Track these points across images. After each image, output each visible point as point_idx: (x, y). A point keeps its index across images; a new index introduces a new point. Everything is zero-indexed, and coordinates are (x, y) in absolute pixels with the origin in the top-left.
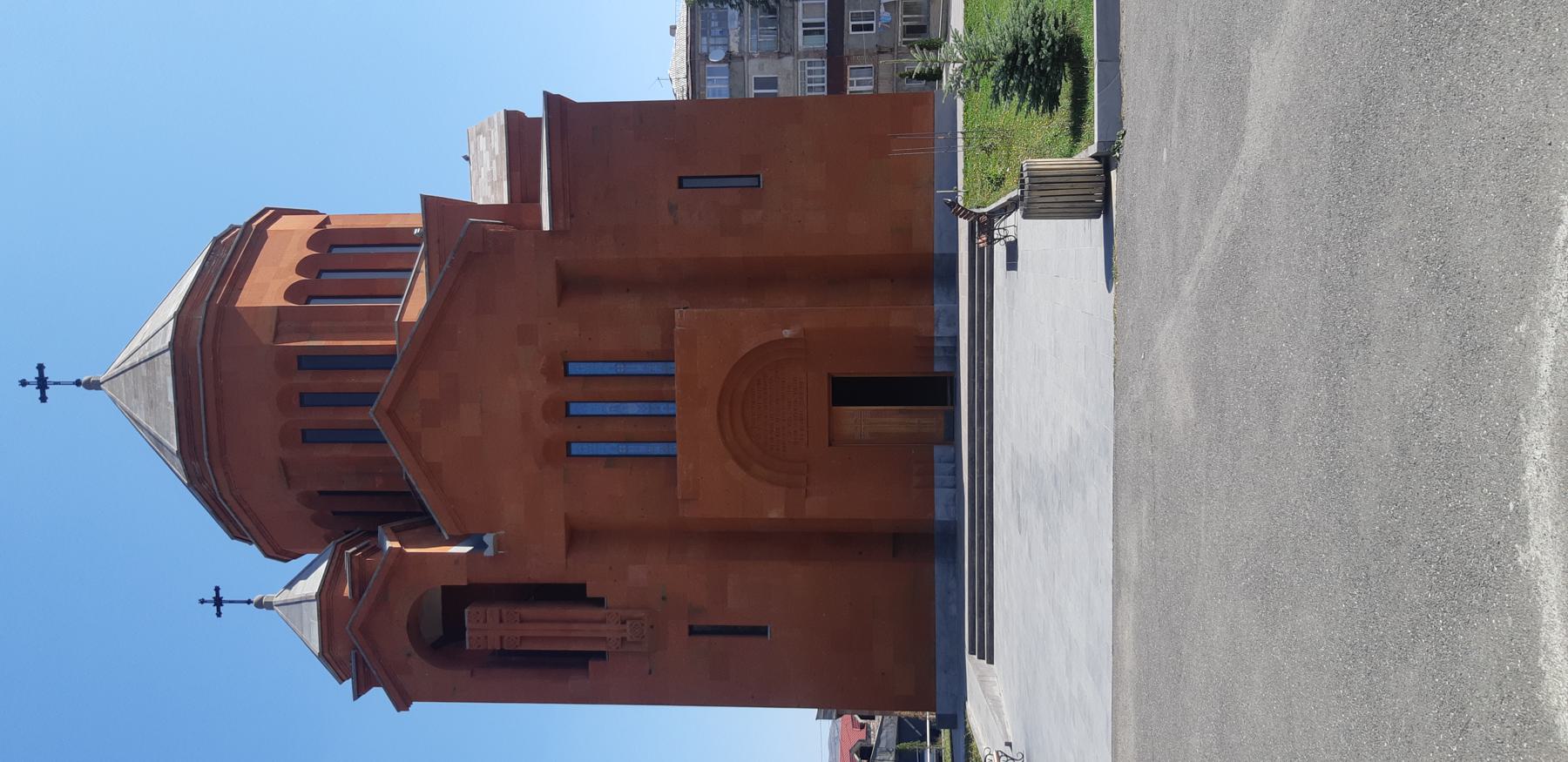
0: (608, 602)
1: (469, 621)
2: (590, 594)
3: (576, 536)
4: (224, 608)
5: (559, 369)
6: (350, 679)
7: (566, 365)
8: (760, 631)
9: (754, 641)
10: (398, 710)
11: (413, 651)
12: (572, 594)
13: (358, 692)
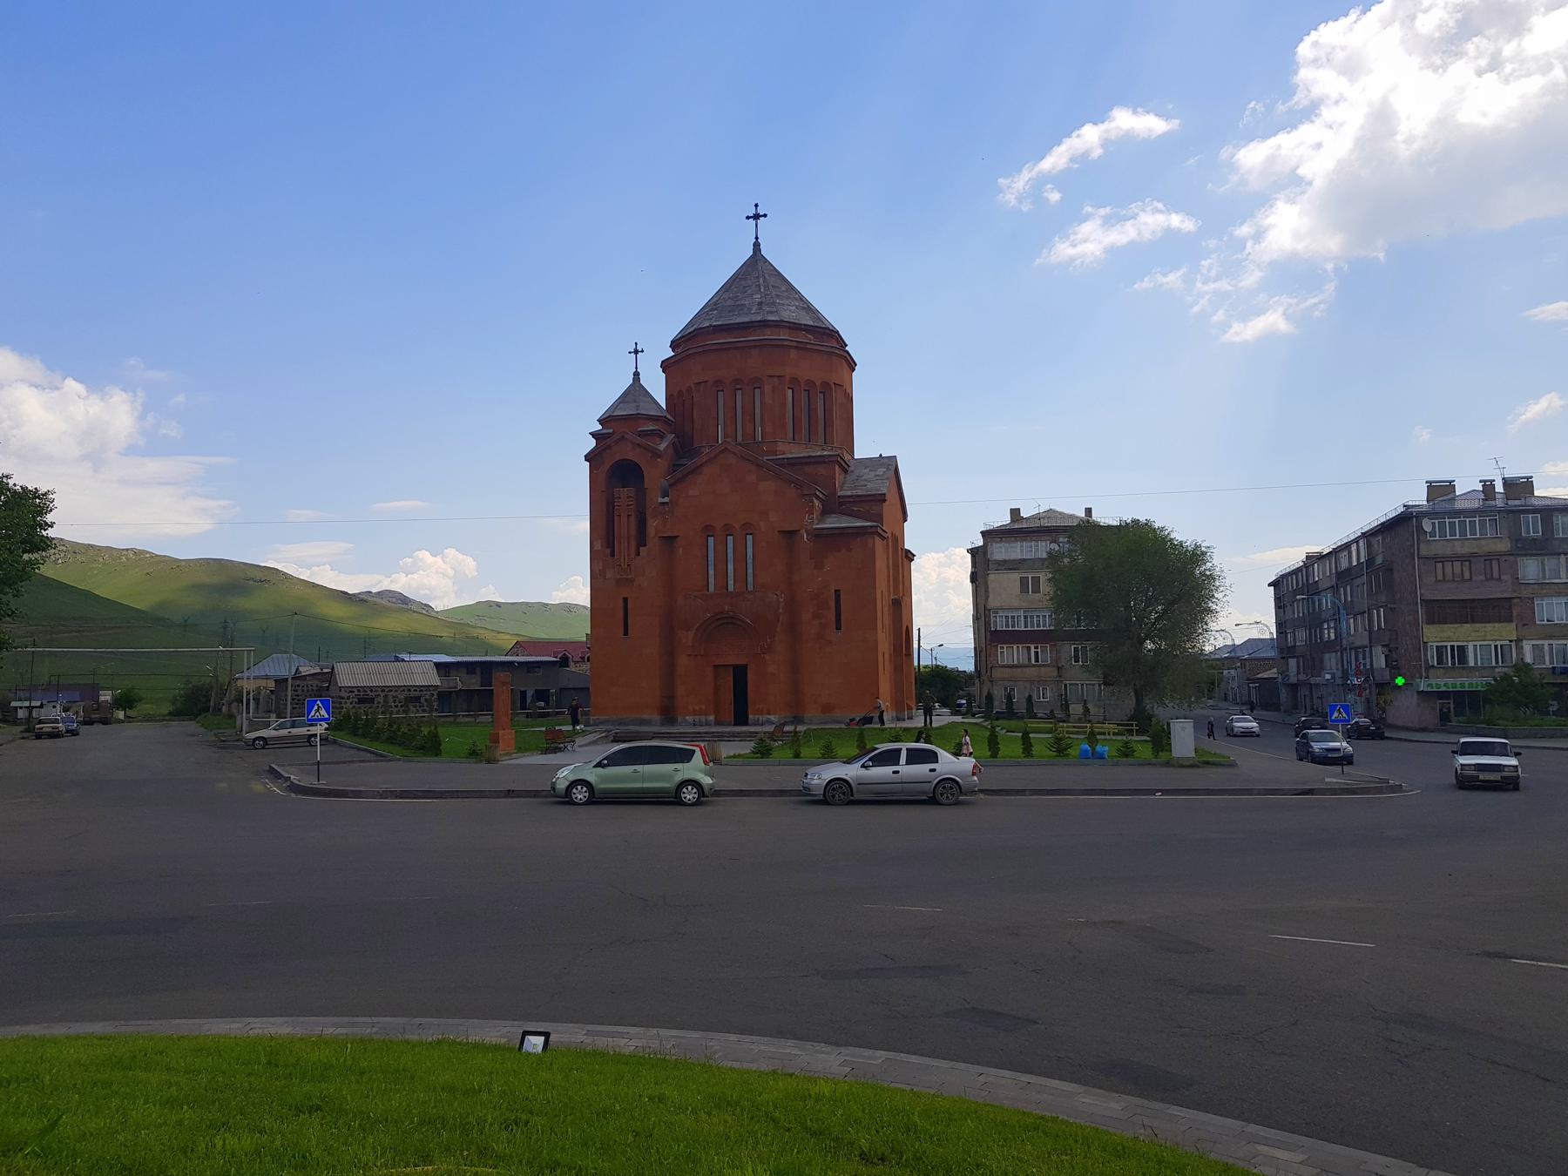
0: (638, 557)
3: (670, 540)
5: (748, 528)
6: (601, 427)
8: (626, 633)
12: (642, 540)
13: (593, 435)
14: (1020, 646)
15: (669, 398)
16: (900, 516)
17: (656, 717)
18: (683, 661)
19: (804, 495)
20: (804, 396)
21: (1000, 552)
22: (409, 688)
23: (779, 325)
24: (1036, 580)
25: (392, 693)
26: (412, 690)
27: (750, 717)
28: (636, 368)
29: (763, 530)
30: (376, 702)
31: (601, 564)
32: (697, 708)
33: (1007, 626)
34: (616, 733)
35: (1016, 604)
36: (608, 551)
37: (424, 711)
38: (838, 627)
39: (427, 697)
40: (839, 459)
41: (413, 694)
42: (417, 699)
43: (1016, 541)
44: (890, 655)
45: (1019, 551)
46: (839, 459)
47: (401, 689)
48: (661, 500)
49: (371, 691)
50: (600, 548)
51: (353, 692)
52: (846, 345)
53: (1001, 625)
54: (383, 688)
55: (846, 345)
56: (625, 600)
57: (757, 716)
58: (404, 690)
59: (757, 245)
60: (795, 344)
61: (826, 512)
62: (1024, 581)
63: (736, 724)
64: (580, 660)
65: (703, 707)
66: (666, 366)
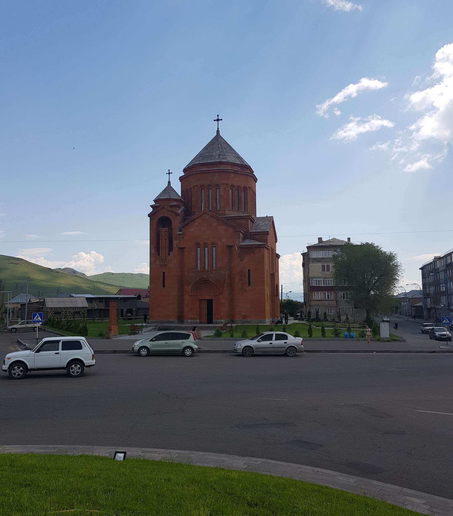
2: (171, 252)
5: (214, 245)
6: (154, 203)
7: (215, 247)
8: (164, 286)
9: (162, 285)
11: (160, 217)
13: (152, 206)
14: (322, 292)
15: (182, 192)
16: (274, 240)
17: (176, 320)
18: (187, 298)
19: (236, 231)
20: (236, 192)
21: (314, 255)
22: (75, 308)
23: (227, 163)
24: (328, 266)
25: (68, 310)
26: (77, 308)
27: (214, 320)
28: (169, 180)
30: (62, 314)
31: (154, 259)
32: (192, 317)
33: (317, 284)
34: (159, 327)
35: (320, 275)
36: (157, 253)
37: (81, 317)
38: (249, 285)
39: (83, 312)
40: (250, 217)
41: (77, 310)
42: (79, 312)
43: (320, 250)
44: (270, 295)
45: (321, 254)
46: (250, 217)
47: (72, 308)
48: (179, 233)
49: (60, 309)
50: (154, 252)
51: (52, 309)
52: (253, 172)
53: (314, 284)
54: (65, 308)
55: (253, 172)
56: (164, 273)
57: (216, 320)
58: (73, 309)
59: (218, 131)
60: (233, 171)
61: (245, 238)
62: (323, 267)
63: (208, 323)
64: (145, 297)
65: (195, 316)
66: (181, 179)
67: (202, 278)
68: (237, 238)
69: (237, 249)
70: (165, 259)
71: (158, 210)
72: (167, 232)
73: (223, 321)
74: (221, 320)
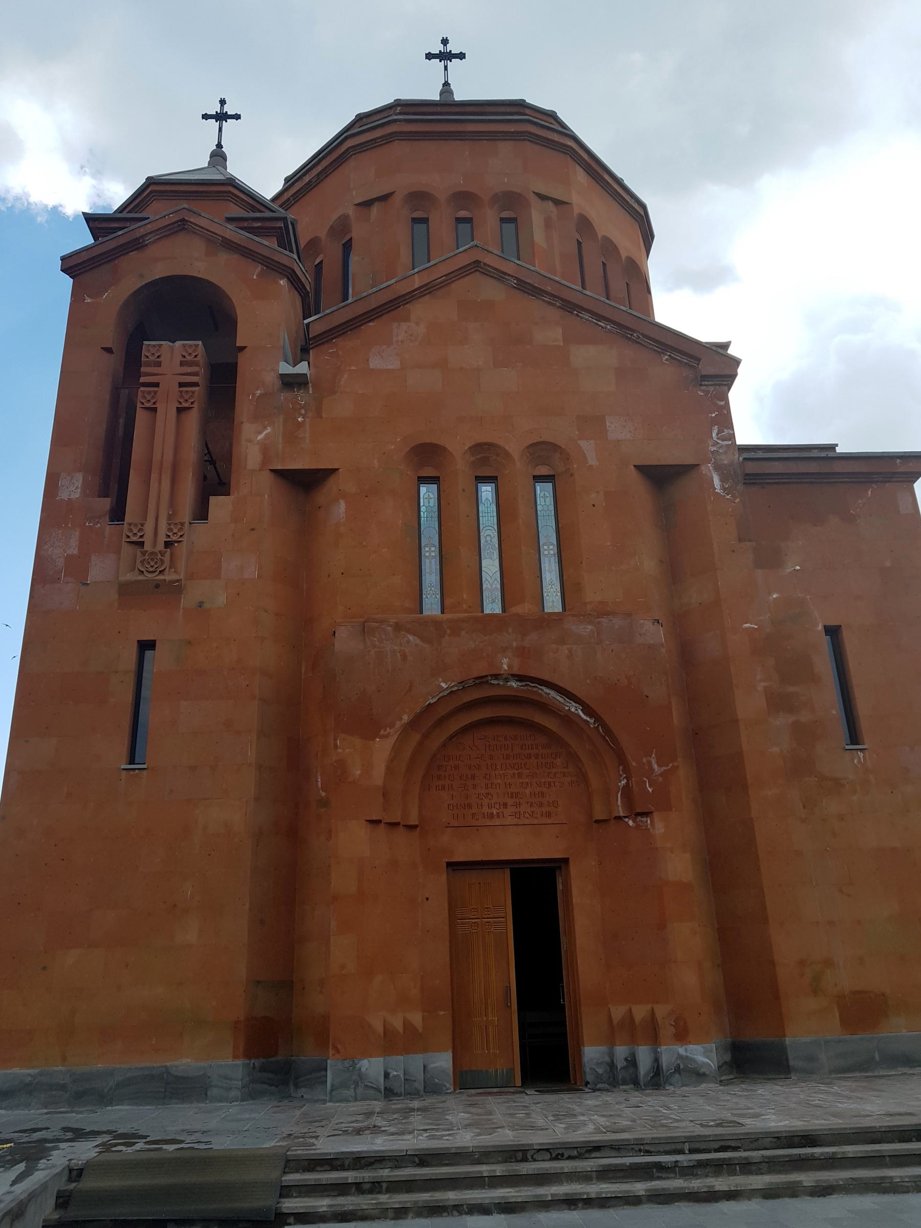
0: (200, 526)
1: (184, 346)
4: (213, 124)
9: (123, 748)
10: (63, 259)
19: (704, 377)
29: (592, 460)
32: (397, 1023)
34: (75, 1173)
36: (106, 504)
38: (854, 737)
50: (76, 495)
65: (417, 1018)
67: (481, 681)
68: (714, 422)
69: (724, 489)
70: (168, 544)
71: (142, 231)
72: (195, 369)
73: (701, 1059)
74: (681, 1051)
